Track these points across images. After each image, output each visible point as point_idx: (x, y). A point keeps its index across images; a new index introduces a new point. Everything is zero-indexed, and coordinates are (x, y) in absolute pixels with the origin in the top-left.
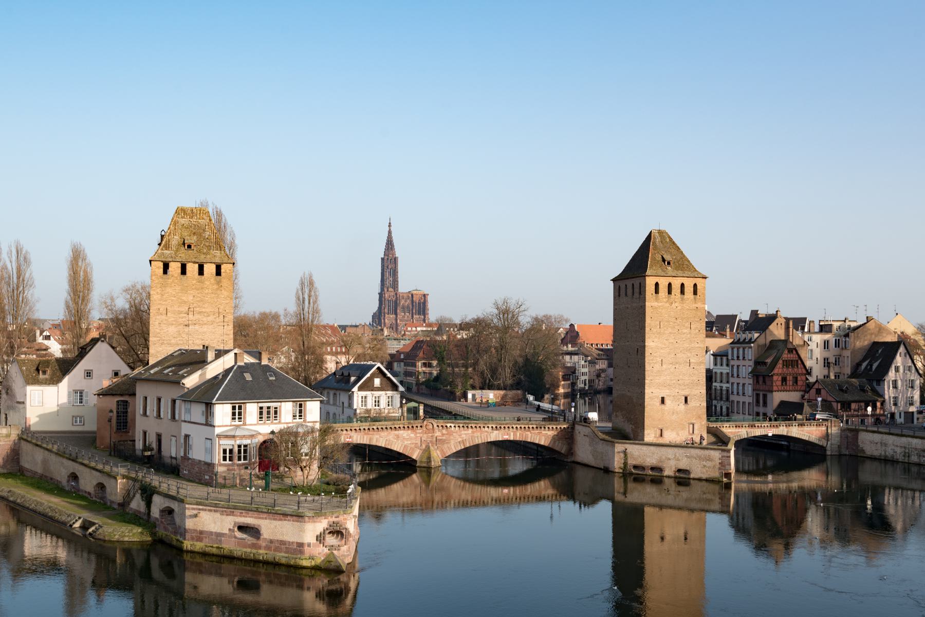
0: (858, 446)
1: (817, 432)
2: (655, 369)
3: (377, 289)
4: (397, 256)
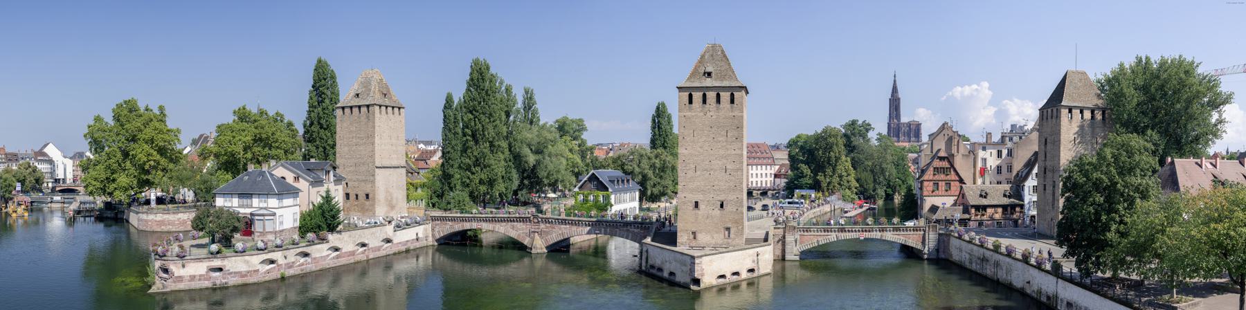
3: (887, 121)
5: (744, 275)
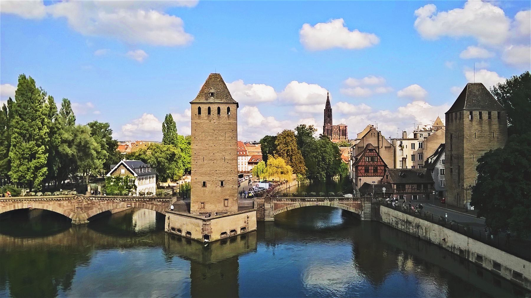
0: (380, 215)
1: (354, 204)
2: (198, 164)
4: (331, 108)
5: (239, 232)
